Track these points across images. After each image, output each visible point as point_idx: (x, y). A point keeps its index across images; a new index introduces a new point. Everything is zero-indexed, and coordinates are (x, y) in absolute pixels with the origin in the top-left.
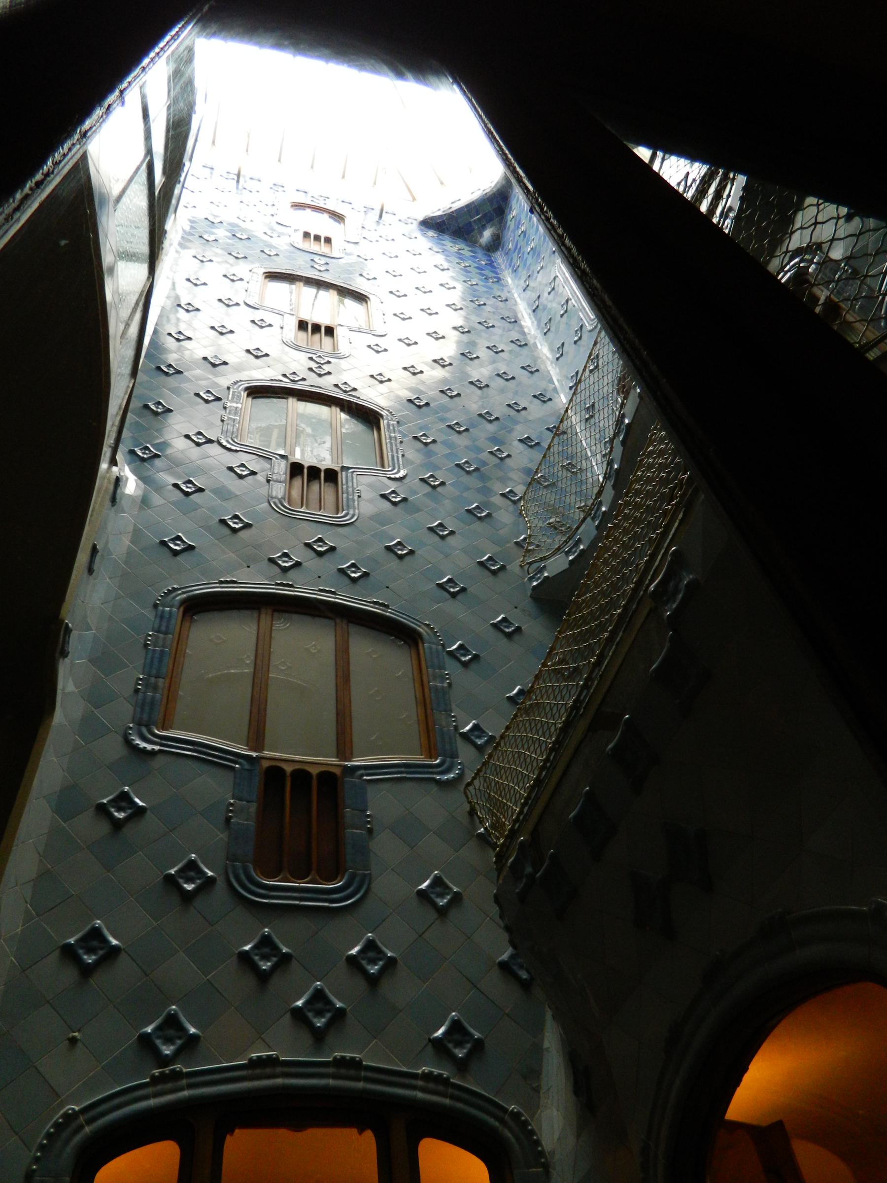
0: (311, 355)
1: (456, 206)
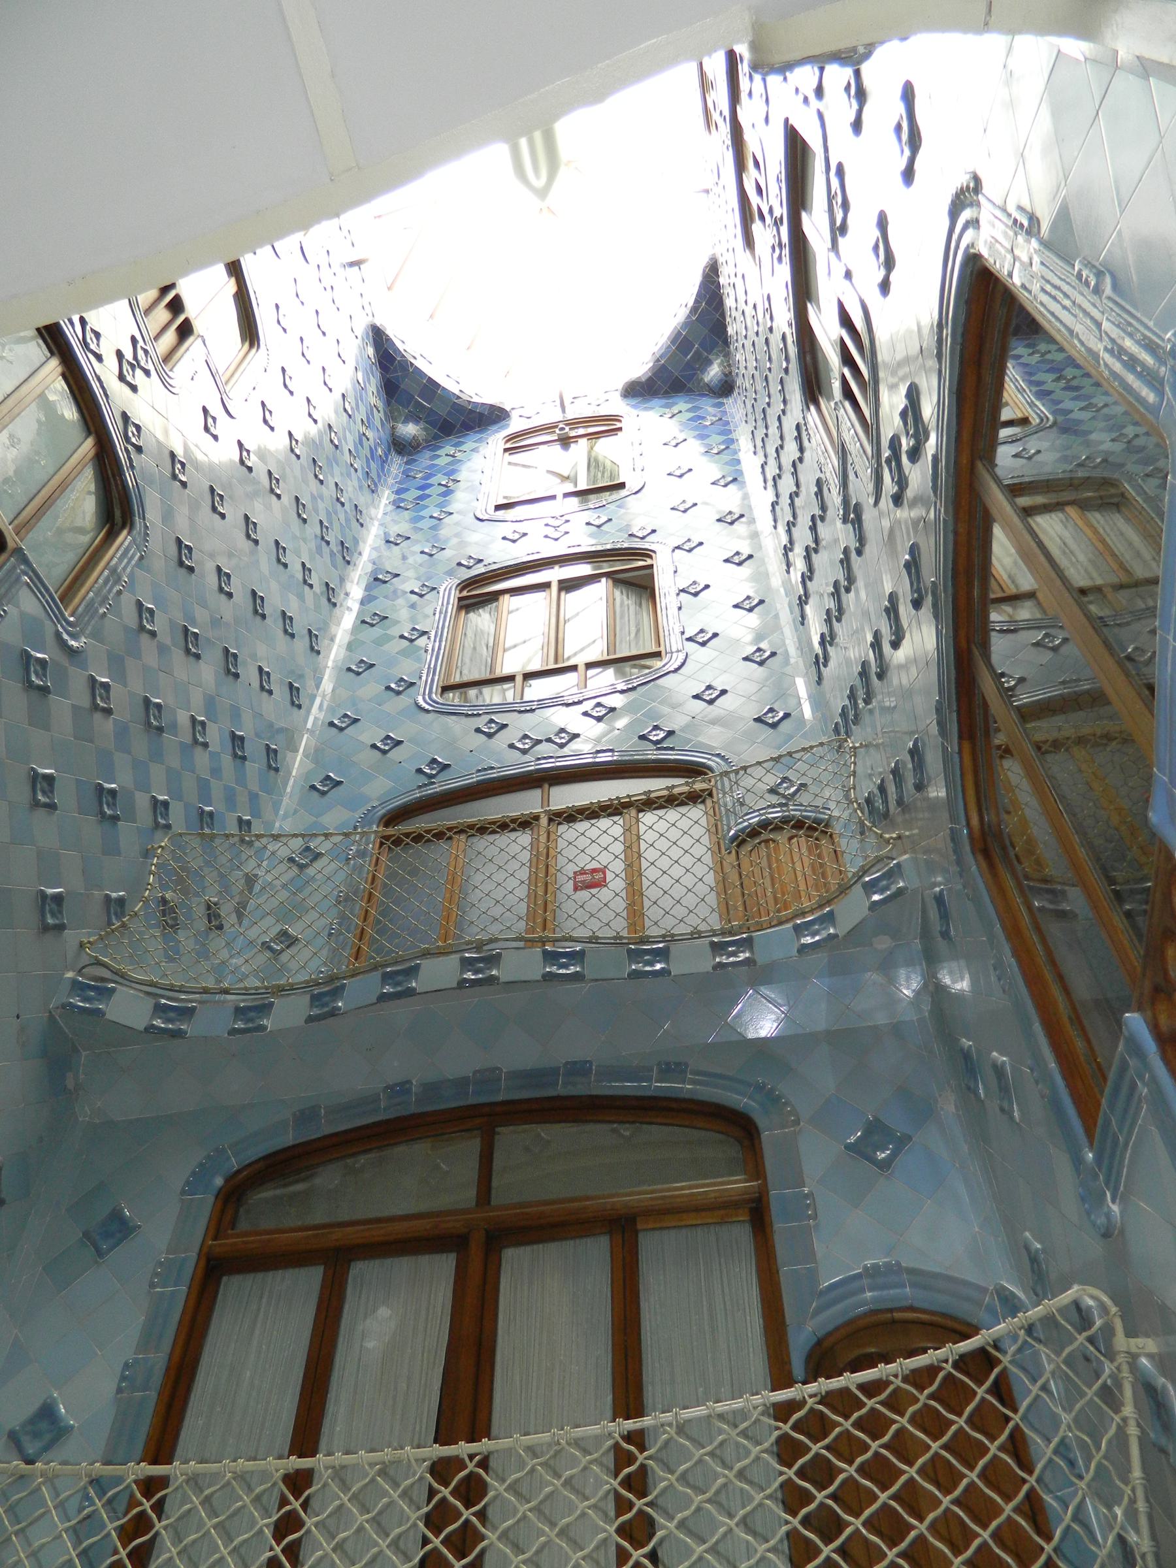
0: (139, 337)
1: (420, 364)
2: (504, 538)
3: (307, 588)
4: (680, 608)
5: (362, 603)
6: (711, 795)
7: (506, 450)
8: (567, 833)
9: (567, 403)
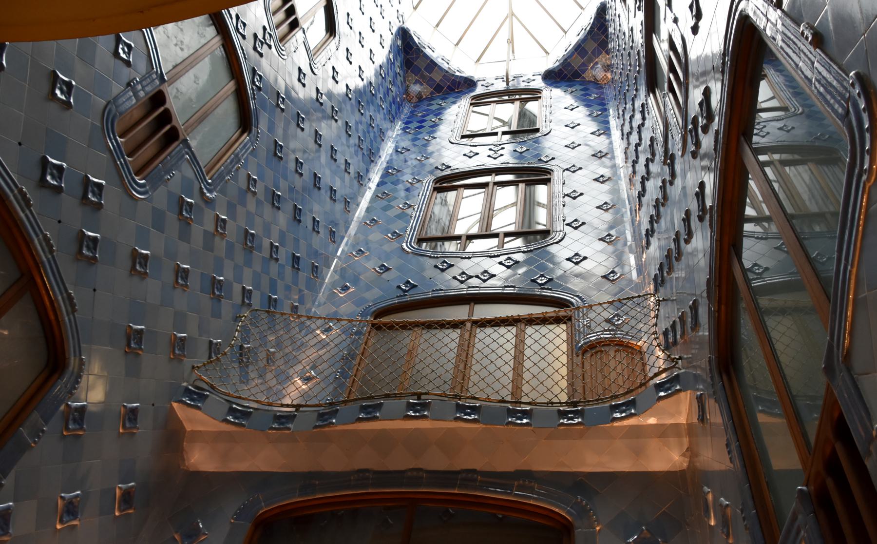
1: (428, 52)
2: (465, 155)
3: (346, 174)
4: (564, 206)
5: (378, 185)
6: (570, 319)
8: (481, 334)
9: (511, 78)
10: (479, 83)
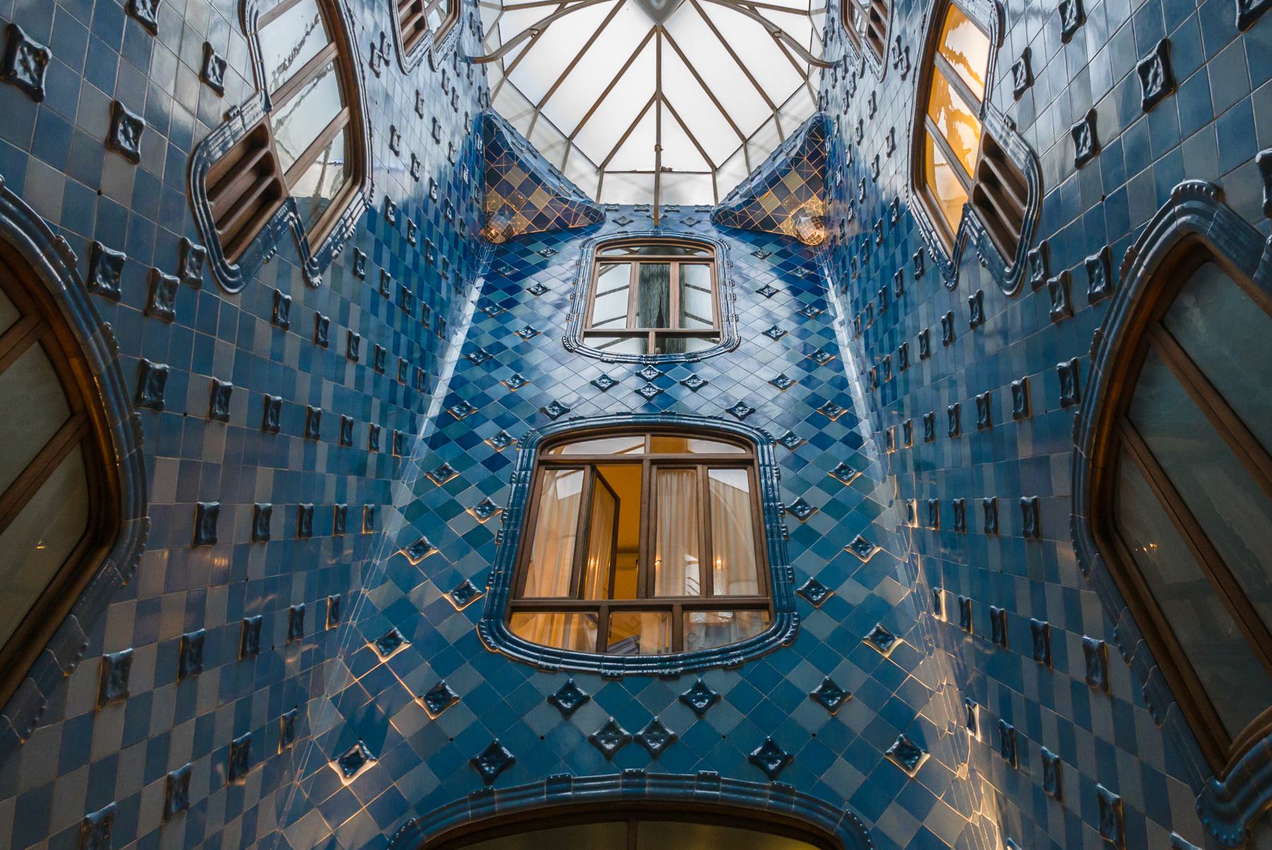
7: (598, 259)
10: (610, 216)
